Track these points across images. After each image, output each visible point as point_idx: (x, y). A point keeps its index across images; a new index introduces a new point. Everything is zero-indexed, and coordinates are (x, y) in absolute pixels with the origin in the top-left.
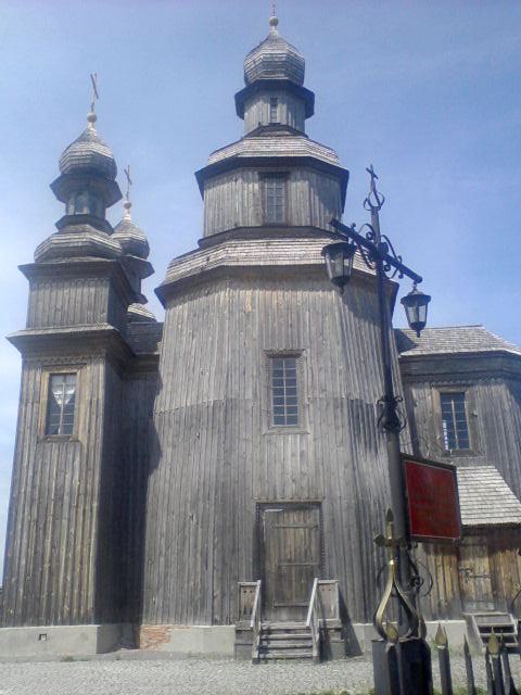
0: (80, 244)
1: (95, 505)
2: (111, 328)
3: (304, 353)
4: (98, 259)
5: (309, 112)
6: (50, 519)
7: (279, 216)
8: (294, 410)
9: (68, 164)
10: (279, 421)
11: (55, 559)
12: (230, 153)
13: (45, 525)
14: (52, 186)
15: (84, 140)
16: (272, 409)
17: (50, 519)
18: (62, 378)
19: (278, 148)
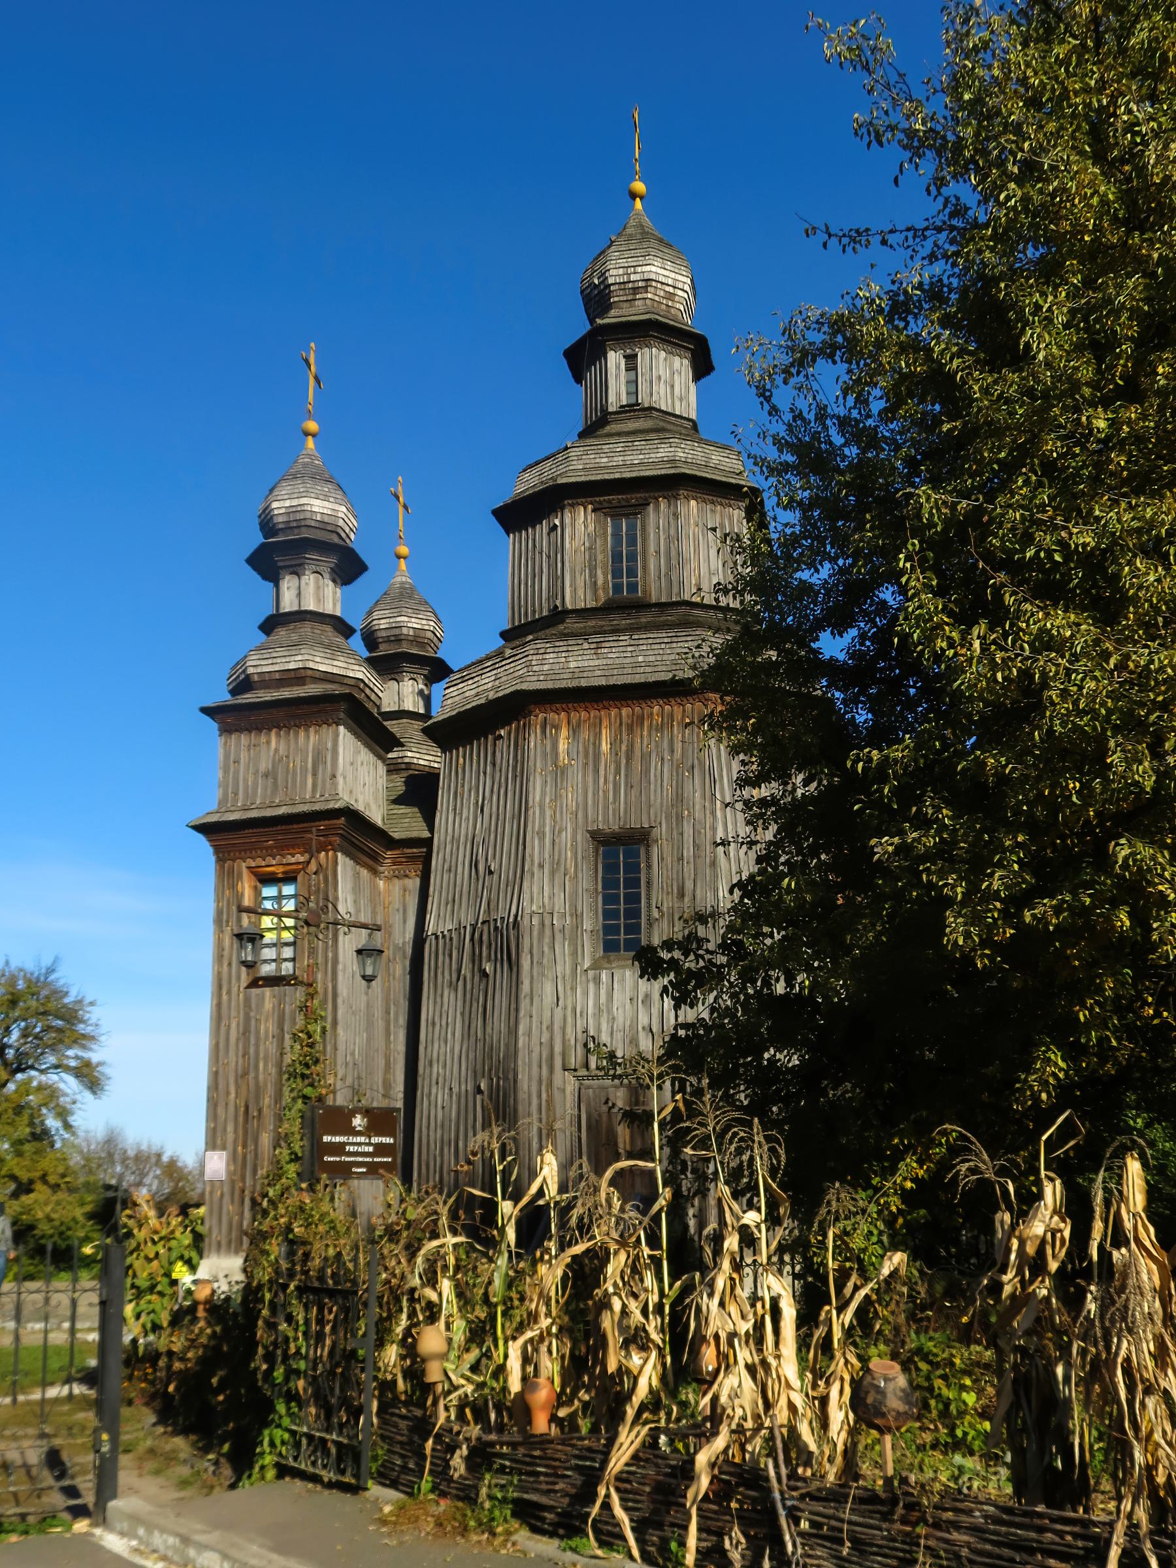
3: (655, 833)
7: (633, 587)
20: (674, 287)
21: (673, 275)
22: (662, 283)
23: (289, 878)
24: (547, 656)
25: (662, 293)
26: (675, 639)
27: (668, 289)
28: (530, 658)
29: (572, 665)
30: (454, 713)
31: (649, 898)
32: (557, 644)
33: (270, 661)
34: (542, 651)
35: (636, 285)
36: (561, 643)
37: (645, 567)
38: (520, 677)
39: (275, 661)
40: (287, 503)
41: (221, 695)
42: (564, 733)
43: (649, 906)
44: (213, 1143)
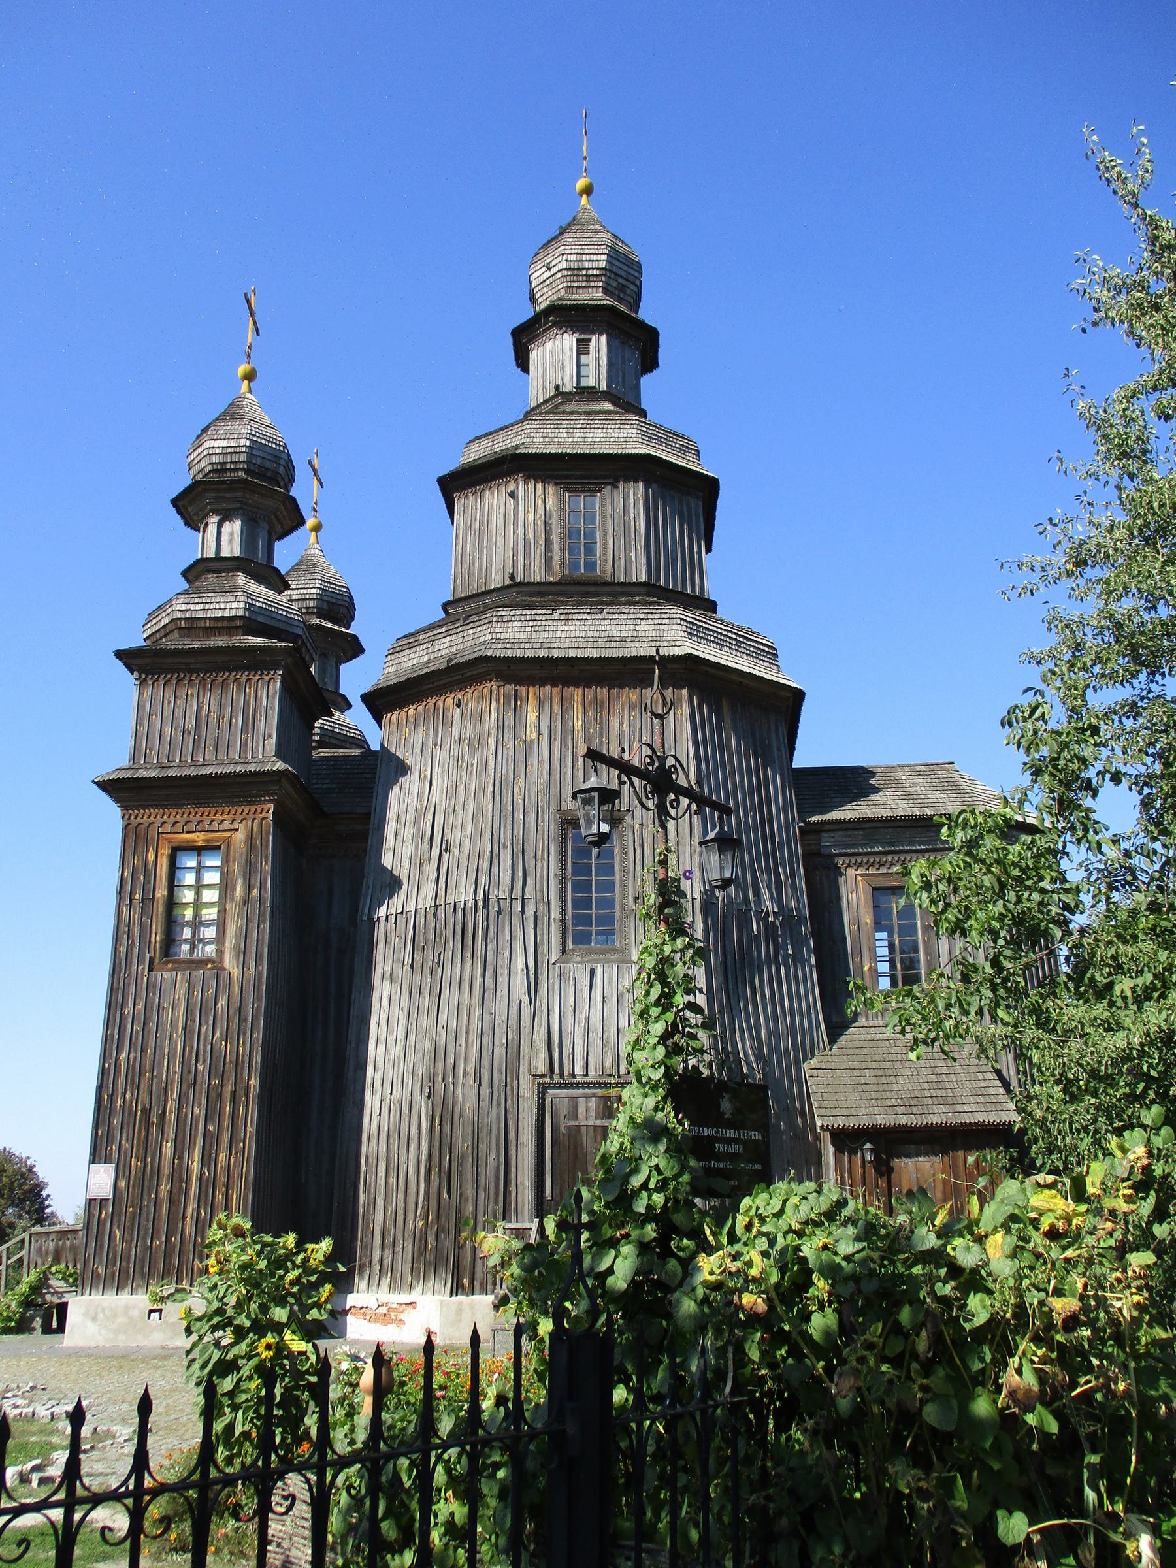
0: (227, 614)
1: (254, 1082)
2: (280, 765)
3: (628, 818)
4: (259, 641)
5: (650, 363)
6: (172, 1105)
7: (590, 565)
8: (610, 919)
9: (204, 463)
10: (582, 938)
11: (179, 1177)
12: (501, 444)
13: (162, 1117)
14: (175, 502)
15: (233, 418)
16: (569, 916)
17: (172, 1105)
18: (196, 853)
19: (589, 437)
20: (627, 280)
21: (625, 268)
22: (616, 274)
23: (211, 848)
24: (510, 624)
25: (615, 284)
26: (650, 616)
27: (620, 280)
28: (494, 624)
29: (541, 635)
30: (403, 679)
31: (624, 885)
32: (524, 612)
33: (201, 606)
34: (505, 619)
35: (590, 272)
36: (529, 612)
37: (604, 548)
38: (484, 643)
39: (207, 607)
40: (224, 443)
41: (136, 639)
42: (532, 705)
43: (624, 895)
44: (97, 1155)
